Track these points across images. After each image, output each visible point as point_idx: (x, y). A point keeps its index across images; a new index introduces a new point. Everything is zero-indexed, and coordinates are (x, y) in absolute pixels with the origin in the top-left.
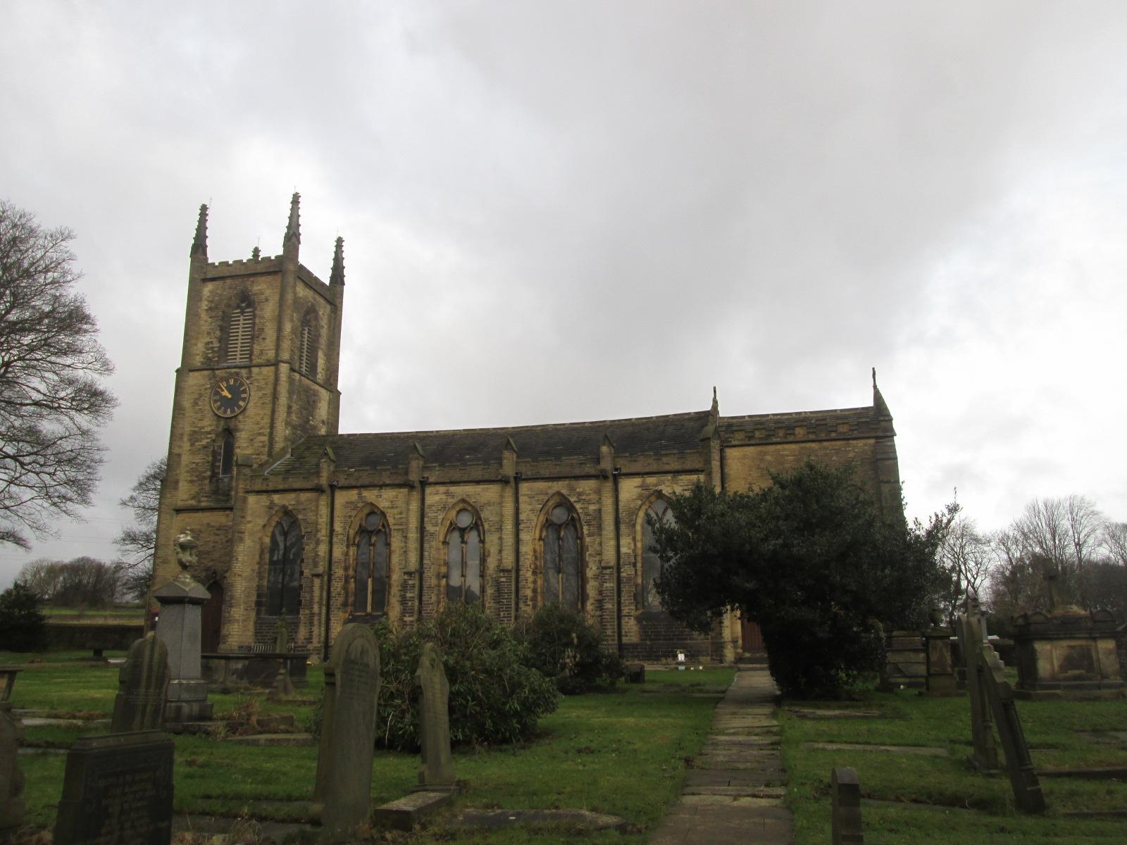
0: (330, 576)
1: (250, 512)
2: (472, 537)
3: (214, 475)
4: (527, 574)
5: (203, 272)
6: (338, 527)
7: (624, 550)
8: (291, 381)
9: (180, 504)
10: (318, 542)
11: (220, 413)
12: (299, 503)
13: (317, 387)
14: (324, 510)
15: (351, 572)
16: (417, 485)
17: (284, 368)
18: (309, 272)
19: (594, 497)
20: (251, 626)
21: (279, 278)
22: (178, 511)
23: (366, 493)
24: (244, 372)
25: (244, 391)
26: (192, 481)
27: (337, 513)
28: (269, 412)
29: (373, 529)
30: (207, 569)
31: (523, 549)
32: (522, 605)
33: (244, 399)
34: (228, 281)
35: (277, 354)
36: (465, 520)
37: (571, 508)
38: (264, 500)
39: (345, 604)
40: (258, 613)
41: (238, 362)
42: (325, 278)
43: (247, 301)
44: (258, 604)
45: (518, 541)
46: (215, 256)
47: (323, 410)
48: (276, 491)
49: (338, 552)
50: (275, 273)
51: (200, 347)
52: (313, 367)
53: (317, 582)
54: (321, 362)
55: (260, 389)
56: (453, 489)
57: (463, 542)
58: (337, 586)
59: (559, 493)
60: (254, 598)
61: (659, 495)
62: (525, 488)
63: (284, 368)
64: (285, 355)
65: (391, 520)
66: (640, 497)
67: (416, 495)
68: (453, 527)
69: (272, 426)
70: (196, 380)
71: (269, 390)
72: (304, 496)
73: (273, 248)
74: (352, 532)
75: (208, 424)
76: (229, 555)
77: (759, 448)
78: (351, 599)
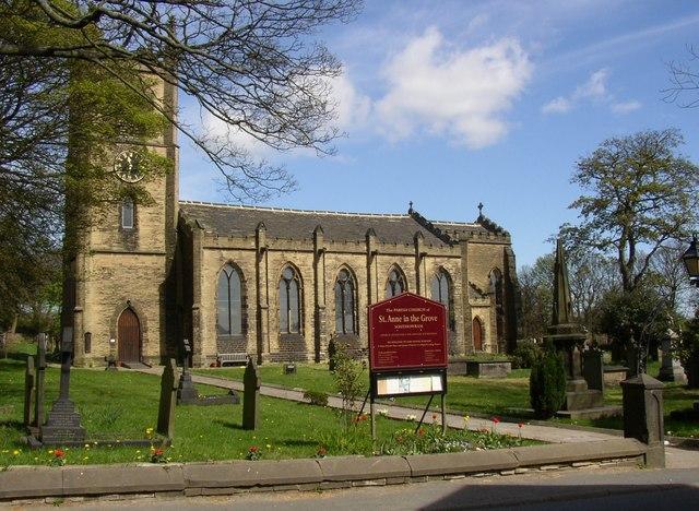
12: (241, 258)
20: (214, 342)
23: (286, 254)
30: (123, 299)
48: (224, 249)
56: (340, 256)
59: (395, 264)
65: (303, 273)
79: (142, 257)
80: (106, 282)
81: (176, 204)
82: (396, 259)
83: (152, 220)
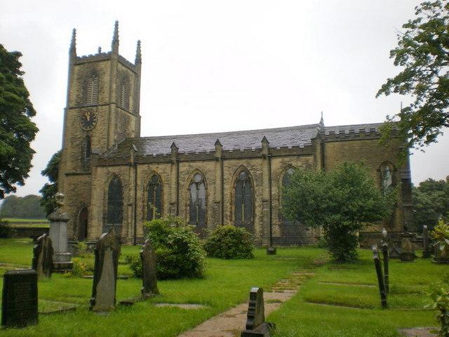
0: (136, 205)
2: (202, 187)
3: (83, 158)
4: (227, 204)
5: (75, 61)
6: (139, 183)
7: (273, 193)
8: (117, 113)
10: (130, 190)
13: (131, 115)
14: (132, 175)
15: (146, 204)
16: (175, 162)
17: (113, 106)
18: (124, 59)
19: (259, 167)
21: (109, 62)
24: (94, 108)
27: (138, 176)
28: (106, 127)
29: (155, 186)
30: (81, 202)
31: (225, 192)
32: (225, 219)
33: (95, 122)
35: (110, 100)
36: (198, 179)
37: (248, 173)
38: (105, 170)
39: (143, 219)
40: (104, 222)
41: (92, 103)
42: (133, 62)
43: (95, 74)
44: (104, 218)
45: (223, 189)
46: (80, 54)
47: (132, 126)
48: (110, 166)
49: (139, 194)
50: (108, 60)
51: (74, 97)
52: (127, 105)
53: (130, 208)
54: (131, 102)
55: (102, 116)
56: (192, 164)
57: (198, 189)
58: (139, 210)
60: (102, 216)
61: (290, 166)
62: (226, 163)
63: (113, 106)
64: (114, 100)
65: (163, 180)
66: (281, 167)
67: (174, 167)
68: (192, 182)
69: (108, 134)
70: (74, 112)
71: (106, 117)
72: (123, 168)
73: (107, 49)
74: (145, 185)
75: (79, 134)
76: (90, 195)
77: (341, 143)
78: (146, 216)
80: (73, 192)
82: (243, 162)
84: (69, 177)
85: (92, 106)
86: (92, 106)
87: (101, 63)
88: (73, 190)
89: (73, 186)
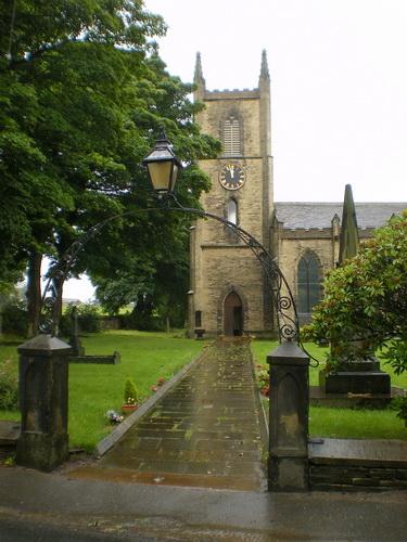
1: (284, 251)
9: (206, 244)
11: (227, 186)
12: (318, 246)
21: (257, 102)
22: (203, 247)
24: (240, 161)
25: (242, 174)
26: (212, 230)
28: (260, 186)
34: (222, 102)
50: (254, 99)
55: (253, 173)
71: (260, 174)
72: (320, 242)
79: (243, 250)
81: (271, 205)
83: (251, 219)
84: (205, 251)
85: (238, 158)
86: (238, 158)
87: (244, 102)
88: (214, 268)
89: (213, 263)
